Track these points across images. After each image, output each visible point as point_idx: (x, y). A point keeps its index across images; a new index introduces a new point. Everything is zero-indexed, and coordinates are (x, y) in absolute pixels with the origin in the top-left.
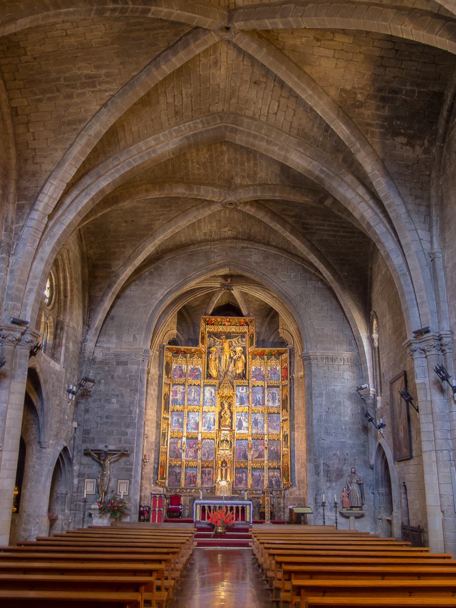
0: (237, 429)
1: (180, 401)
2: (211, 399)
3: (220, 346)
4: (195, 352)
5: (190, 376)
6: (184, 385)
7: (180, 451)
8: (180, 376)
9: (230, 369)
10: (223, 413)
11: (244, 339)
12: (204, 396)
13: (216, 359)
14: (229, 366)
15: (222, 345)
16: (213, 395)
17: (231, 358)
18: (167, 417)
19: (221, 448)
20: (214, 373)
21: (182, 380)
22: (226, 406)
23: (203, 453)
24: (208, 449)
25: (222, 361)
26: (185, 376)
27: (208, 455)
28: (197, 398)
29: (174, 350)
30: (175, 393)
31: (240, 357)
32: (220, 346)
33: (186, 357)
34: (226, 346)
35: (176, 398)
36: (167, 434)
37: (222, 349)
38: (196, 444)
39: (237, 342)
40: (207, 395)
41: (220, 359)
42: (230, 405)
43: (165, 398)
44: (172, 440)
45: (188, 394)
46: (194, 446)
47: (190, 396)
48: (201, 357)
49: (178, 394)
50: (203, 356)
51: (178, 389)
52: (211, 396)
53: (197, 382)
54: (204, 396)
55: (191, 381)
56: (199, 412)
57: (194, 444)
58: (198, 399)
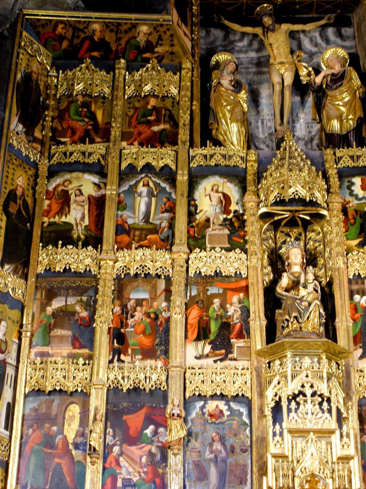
0: (360, 352)
1: (79, 232)
2: (228, 223)
3: (253, 55)
4: (150, 47)
5: (126, 136)
6: (100, 170)
7: (77, 454)
8: (86, 137)
9: (301, 129)
10: (285, 281)
11: (347, 31)
12: (191, 215)
13: (237, 86)
14: (293, 121)
15: (259, 50)
16: (233, 207)
17: (300, 88)
18: (19, 295)
19: (293, 426)
20: (232, 132)
21: (97, 149)
22: (295, 256)
23: (190, 466)
24: (218, 446)
25: (264, 101)
26: (106, 137)
27: (222, 476)
28: (160, 219)
29: (61, 38)
30: (64, 200)
31: (337, 79)
32: (253, 55)
33: (111, 69)
34: (278, 42)
35: (63, 219)
36: (10, 371)
37: (263, 64)
38: (158, 419)
39: (319, 40)
40: (207, 205)
41: (254, 98)
42: (311, 259)
43: (13, 209)
44: (33, 403)
45: (121, 205)
46: (149, 431)
47: (126, 214)
48: (177, 69)
49: (73, 206)
50: (187, 65)
51: (75, 184)
52: (226, 211)
53: (163, 157)
54: (191, 215)
55: (134, 154)
56: (168, 280)
57: (149, 420)
58: (165, 224)
